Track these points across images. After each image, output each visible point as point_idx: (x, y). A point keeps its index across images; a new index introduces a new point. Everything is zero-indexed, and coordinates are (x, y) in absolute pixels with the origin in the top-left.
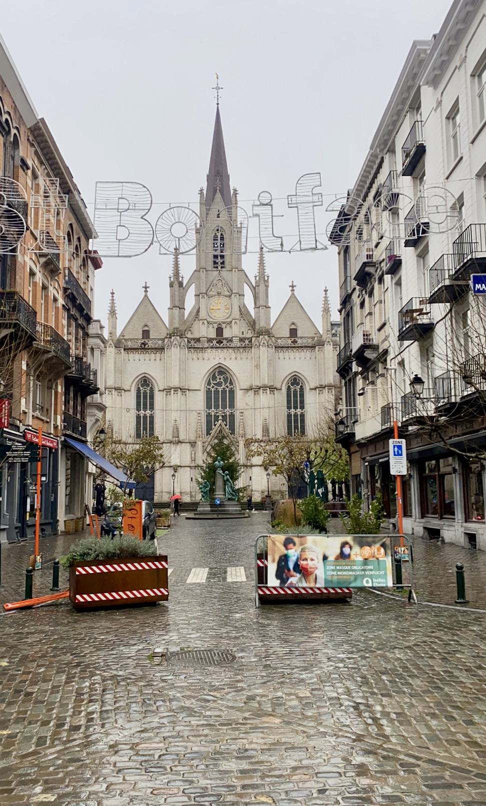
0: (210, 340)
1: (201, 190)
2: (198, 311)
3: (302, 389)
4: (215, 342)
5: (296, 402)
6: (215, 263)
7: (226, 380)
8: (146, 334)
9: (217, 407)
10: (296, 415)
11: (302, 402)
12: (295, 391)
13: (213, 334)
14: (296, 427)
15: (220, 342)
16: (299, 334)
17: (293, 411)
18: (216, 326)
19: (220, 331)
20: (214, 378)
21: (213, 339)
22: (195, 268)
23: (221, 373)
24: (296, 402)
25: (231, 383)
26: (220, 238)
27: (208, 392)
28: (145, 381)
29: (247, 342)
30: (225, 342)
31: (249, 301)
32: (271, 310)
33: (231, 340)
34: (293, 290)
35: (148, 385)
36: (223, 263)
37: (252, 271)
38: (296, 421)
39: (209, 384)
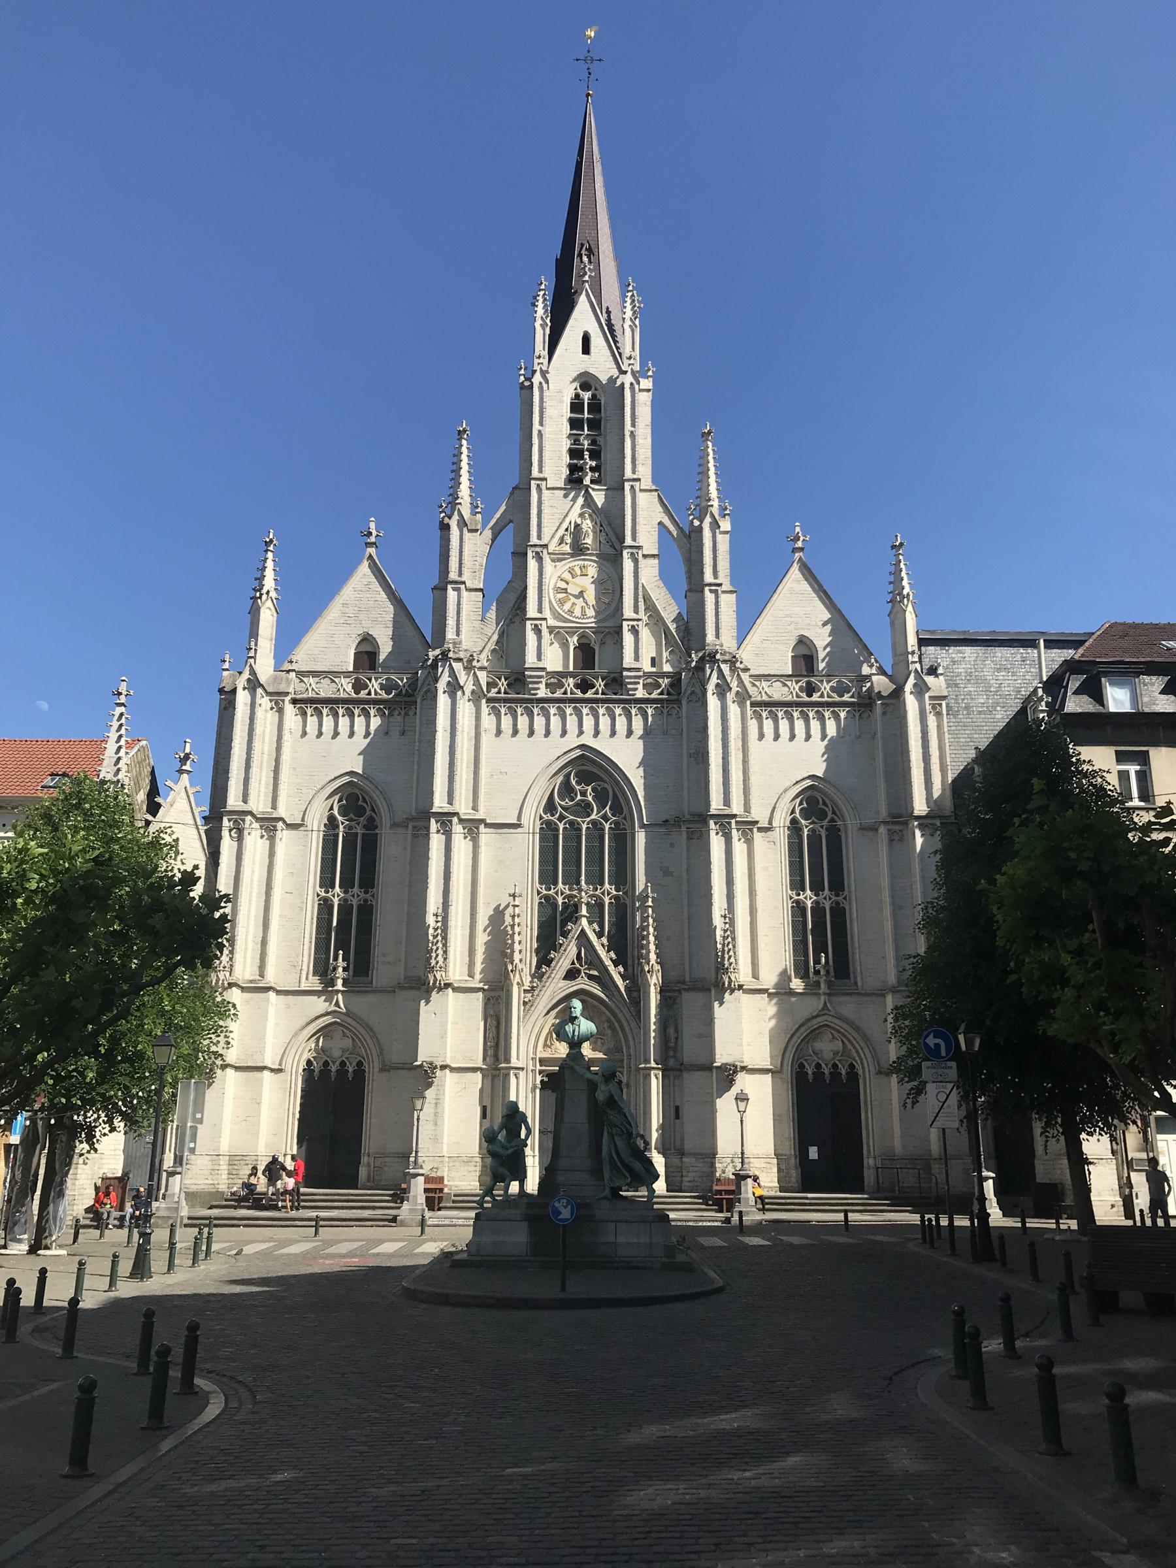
6: (573, 468)
9: (572, 879)
18: (574, 641)
20: (566, 789)
23: (584, 778)
27: (548, 833)
39: (550, 806)
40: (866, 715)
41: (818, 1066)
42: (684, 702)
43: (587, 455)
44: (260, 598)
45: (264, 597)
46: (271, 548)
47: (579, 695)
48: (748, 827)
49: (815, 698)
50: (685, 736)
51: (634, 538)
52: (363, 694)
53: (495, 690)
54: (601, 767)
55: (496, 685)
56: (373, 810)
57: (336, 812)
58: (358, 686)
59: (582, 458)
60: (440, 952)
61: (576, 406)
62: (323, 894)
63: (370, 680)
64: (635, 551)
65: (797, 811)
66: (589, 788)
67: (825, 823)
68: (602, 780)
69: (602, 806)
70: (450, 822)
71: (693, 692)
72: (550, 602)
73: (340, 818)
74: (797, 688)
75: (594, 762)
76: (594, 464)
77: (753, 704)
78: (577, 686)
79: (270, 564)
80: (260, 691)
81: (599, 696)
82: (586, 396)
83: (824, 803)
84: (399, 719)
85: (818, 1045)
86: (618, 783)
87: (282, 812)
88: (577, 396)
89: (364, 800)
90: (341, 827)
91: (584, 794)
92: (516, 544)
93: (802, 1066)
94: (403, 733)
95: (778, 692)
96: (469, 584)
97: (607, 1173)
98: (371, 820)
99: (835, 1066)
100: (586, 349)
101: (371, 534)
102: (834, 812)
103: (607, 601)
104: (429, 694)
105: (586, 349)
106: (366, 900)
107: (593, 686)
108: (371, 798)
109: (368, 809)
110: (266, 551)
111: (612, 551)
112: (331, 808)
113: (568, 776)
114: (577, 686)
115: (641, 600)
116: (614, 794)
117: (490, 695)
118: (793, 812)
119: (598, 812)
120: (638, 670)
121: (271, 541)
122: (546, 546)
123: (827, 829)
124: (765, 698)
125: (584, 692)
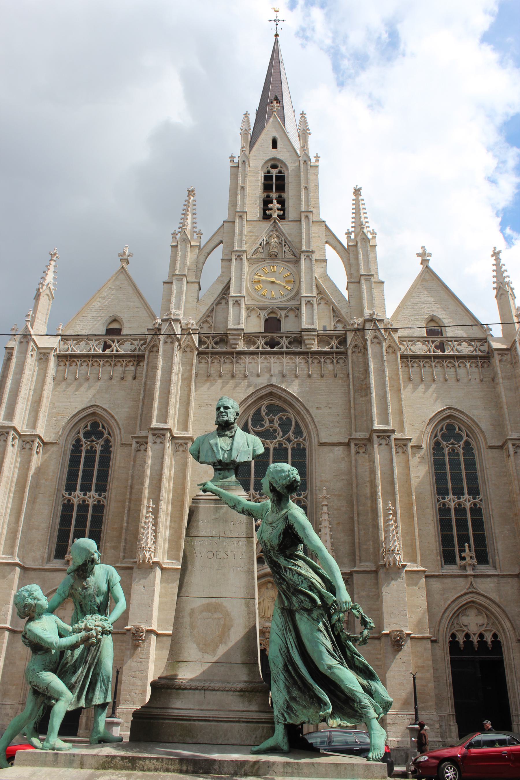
0: (250, 338)
1: (246, 115)
2: (227, 287)
3: (468, 448)
4: (261, 342)
5: (457, 479)
7: (285, 425)
8: (113, 332)
10: (460, 510)
11: (473, 479)
12: (453, 454)
13: (255, 325)
14: (463, 539)
15: (272, 344)
16: (449, 333)
17: (451, 501)
18: (264, 315)
19: (272, 323)
21: (257, 335)
22: (225, 218)
23: (273, 409)
24: (457, 479)
25: (298, 432)
26: (275, 183)
28: (95, 425)
29: (334, 343)
30: (284, 342)
31: (337, 272)
32: (385, 286)
33: (297, 339)
34: (425, 262)
35: (100, 435)
36: (283, 209)
37: (341, 226)
38: (462, 524)
40: (486, 365)
41: (467, 636)
42: (350, 352)
43: (275, 201)
44: (42, 288)
45: (45, 287)
46: (55, 258)
47: (268, 349)
48: (403, 444)
49: (446, 353)
50: (351, 376)
51: (309, 245)
52: (108, 351)
53: (203, 347)
54: (285, 401)
55: (205, 343)
56: (109, 434)
57: (81, 436)
58: (106, 346)
59: (271, 202)
60: (150, 536)
61: (268, 178)
62: (67, 496)
63: (113, 342)
64: (309, 254)
65: (439, 435)
66: (276, 418)
67: (462, 443)
68: (285, 410)
69: (285, 432)
70: (164, 435)
71: (356, 346)
72: (247, 289)
73: (83, 440)
74: (433, 346)
75: (280, 398)
76: (279, 206)
77: (402, 357)
78: (266, 344)
79: (52, 268)
80: (32, 343)
81: (284, 349)
82: (274, 172)
83: (460, 429)
84: (133, 368)
85: (464, 620)
86: (299, 413)
87: (40, 431)
88: (269, 172)
89: (104, 427)
90: (84, 446)
91: (271, 422)
92: (224, 254)
93: (453, 636)
94: (134, 378)
95: (419, 349)
96: (190, 279)
97: (278, 695)
98: (107, 441)
99: (481, 636)
100: (274, 144)
101: (124, 253)
102: (467, 436)
103: (290, 288)
104: (155, 349)
105: (274, 144)
106: (99, 501)
107: (278, 343)
108: (109, 424)
109: (106, 433)
110: (51, 260)
111: (294, 258)
112: (79, 433)
113: (259, 410)
114: (266, 344)
115: (314, 287)
116: (297, 425)
117: (200, 349)
118: (436, 436)
119: (283, 435)
120: (314, 330)
121: (55, 254)
122: (245, 251)
123: (463, 448)
124: (410, 353)
125: (272, 347)
